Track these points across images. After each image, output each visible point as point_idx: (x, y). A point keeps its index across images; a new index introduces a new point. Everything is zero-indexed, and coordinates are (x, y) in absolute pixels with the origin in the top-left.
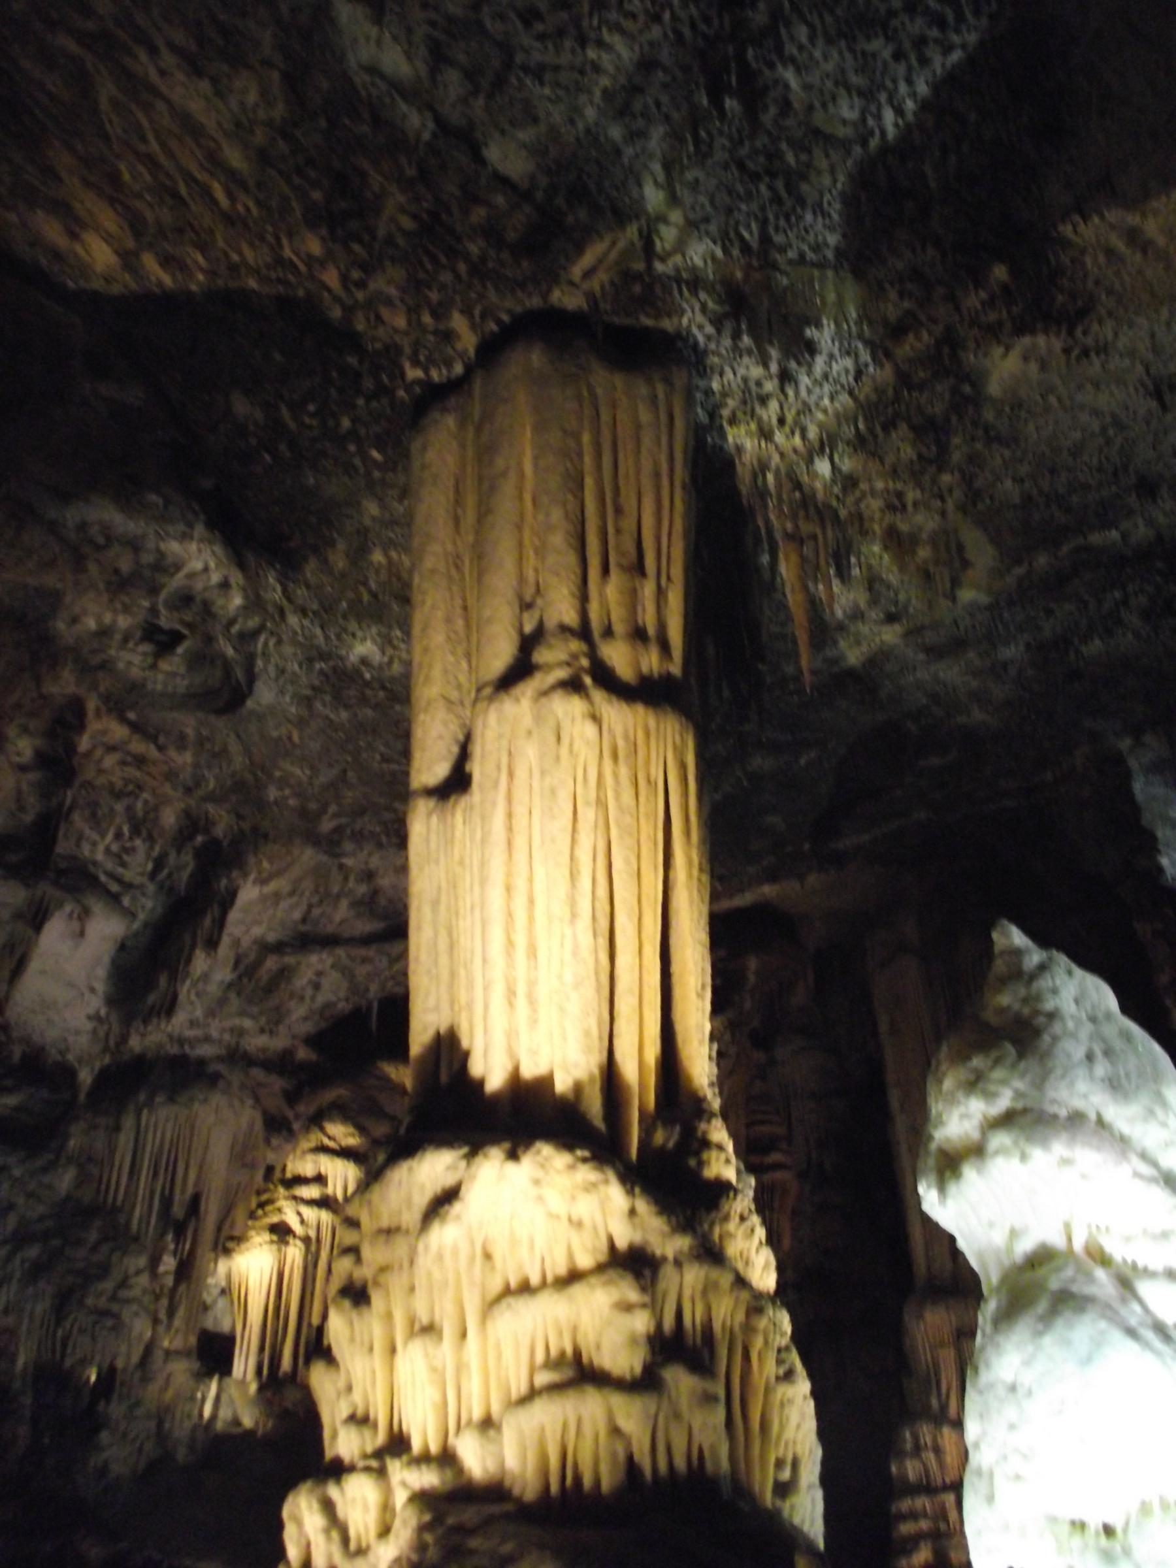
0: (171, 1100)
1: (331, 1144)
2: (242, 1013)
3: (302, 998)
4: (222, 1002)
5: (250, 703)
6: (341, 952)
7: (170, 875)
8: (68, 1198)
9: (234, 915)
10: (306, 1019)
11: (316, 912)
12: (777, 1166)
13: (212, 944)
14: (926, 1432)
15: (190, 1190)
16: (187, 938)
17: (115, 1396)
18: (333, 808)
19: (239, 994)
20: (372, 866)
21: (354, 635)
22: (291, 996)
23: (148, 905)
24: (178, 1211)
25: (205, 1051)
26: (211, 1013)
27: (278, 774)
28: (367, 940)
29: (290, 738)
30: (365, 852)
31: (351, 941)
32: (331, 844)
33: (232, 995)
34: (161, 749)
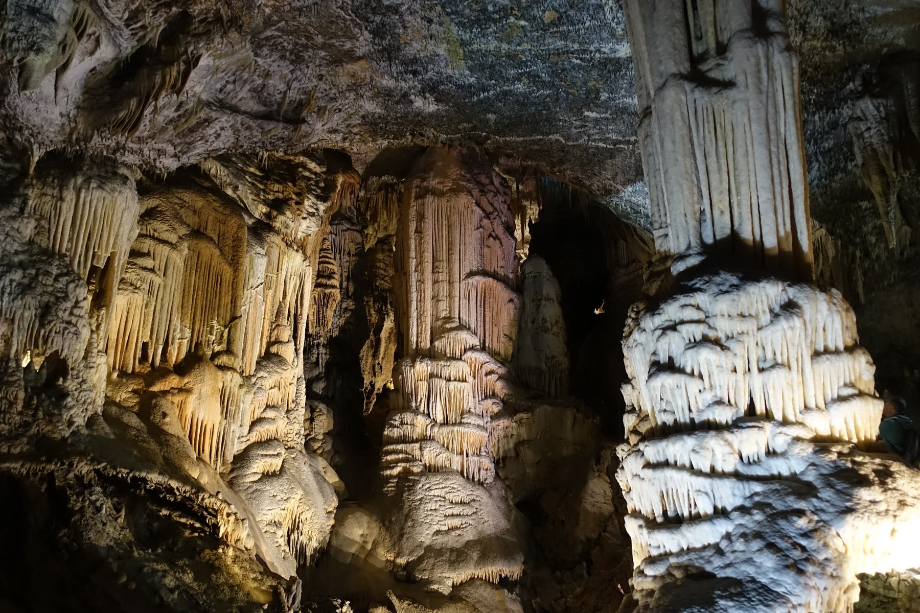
0: (100, 187)
1: (156, 235)
2: (170, 141)
4: (163, 130)
6: (240, 118)
7: (143, 27)
8: (31, 242)
9: (192, 74)
10: (199, 155)
11: (230, 87)
12: (333, 287)
14: (408, 417)
15: (110, 250)
16: (158, 79)
17: (69, 377)
19: (175, 129)
20: (271, 69)
22: (202, 138)
23: (128, 46)
24: (101, 265)
26: (152, 137)
28: (255, 116)
30: (272, 59)
31: (245, 113)
32: (257, 47)
33: (171, 127)
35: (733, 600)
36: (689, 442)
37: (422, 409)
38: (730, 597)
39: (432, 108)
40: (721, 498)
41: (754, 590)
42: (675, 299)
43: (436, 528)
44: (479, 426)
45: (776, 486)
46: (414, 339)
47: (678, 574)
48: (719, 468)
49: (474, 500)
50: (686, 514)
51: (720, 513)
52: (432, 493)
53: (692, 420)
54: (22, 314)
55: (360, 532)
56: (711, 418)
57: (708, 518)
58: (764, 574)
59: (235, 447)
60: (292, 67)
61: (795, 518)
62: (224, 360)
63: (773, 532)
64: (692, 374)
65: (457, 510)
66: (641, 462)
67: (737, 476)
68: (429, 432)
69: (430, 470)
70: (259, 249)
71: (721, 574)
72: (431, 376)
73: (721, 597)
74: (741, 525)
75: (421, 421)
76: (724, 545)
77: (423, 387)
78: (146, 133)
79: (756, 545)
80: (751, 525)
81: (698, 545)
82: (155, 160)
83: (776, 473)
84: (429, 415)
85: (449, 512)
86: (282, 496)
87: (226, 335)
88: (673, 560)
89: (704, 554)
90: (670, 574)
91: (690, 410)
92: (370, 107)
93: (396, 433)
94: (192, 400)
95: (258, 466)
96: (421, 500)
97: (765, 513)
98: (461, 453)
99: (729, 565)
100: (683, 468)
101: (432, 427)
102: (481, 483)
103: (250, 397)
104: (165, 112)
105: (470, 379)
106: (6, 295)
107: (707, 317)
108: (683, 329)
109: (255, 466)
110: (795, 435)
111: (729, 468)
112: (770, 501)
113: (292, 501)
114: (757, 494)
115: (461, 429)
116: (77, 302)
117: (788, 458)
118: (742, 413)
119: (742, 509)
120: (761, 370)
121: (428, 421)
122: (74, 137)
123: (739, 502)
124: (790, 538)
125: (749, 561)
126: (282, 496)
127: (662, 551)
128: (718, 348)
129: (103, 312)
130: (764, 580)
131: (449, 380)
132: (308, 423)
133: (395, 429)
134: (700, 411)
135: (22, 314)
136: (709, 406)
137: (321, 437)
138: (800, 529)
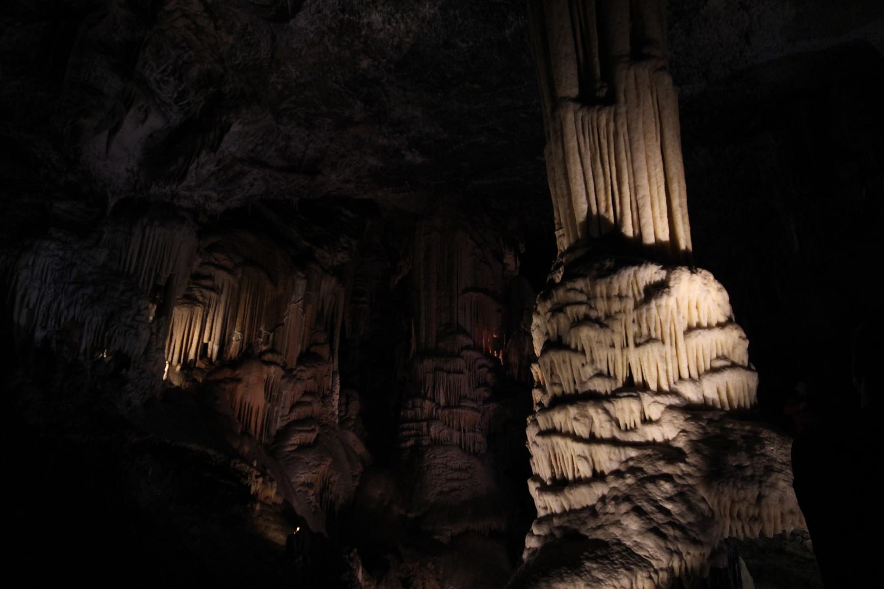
1: (216, 262)
3: (244, 189)
5: (291, 23)
7: (188, 104)
9: (226, 138)
11: (259, 148)
13: (214, 149)
14: (418, 401)
18: (293, 98)
21: (376, 7)
23: (176, 117)
24: (162, 283)
25: (184, 203)
27: (282, 68)
29: (301, 51)
34: (217, 28)
35: (597, 562)
37: (429, 395)
38: (595, 560)
39: (420, 160)
40: (599, 462)
41: (619, 552)
43: (439, 489)
44: (473, 409)
45: (649, 452)
46: (424, 341)
47: (557, 533)
48: (598, 435)
49: (470, 467)
50: (570, 477)
51: (598, 476)
52: (436, 461)
53: (576, 391)
54: (91, 320)
55: (379, 492)
56: (592, 388)
58: (629, 537)
59: (279, 424)
60: (307, 132)
61: (662, 482)
62: (268, 357)
63: (641, 495)
64: (575, 350)
65: (455, 475)
66: (536, 431)
67: (614, 442)
68: (434, 413)
69: (436, 443)
70: (300, 274)
71: (593, 536)
72: (436, 369)
73: (588, 559)
74: (614, 488)
75: (427, 404)
76: (599, 507)
77: (430, 376)
78: (193, 183)
79: (625, 507)
80: (623, 488)
81: (578, 507)
82: (204, 204)
83: (650, 439)
84: (434, 400)
85: (449, 476)
86: (314, 462)
87: (271, 338)
88: (556, 522)
89: (581, 515)
90: (551, 534)
91: (575, 383)
92: (373, 161)
93: (410, 414)
94: (240, 388)
95: (296, 439)
96: (428, 466)
97: (636, 476)
98: (460, 430)
101: (437, 410)
102: (475, 454)
103: (291, 385)
104: (208, 167)
105: (466, 371)
106: (78, 305)
107: (589, 299)
108: (568, 310)
109: (293, 439)
110: (668, 403)
111: (606, 434)
112: (642, 466)
113: (323, 467)
114: (632, 459)
115: (460, 411)
116: (139, 311)
117: (661, 425)
118: (620, 384)
119: (618, 474)
120: (637, 345)
121: (434, 405)
122: (138, 187)
123: (615, 466)
124: (656, 501)
125: (617, 523)
126: (314, 462)
127: (549, 512)
128: (597, 326)
129: (163, 319)
131: (449, 372)
132: (343, 408)
133: (409, 412)
135: (91, 320)
136: (591, 378)
137: (354, 417)
138: (667, 493)
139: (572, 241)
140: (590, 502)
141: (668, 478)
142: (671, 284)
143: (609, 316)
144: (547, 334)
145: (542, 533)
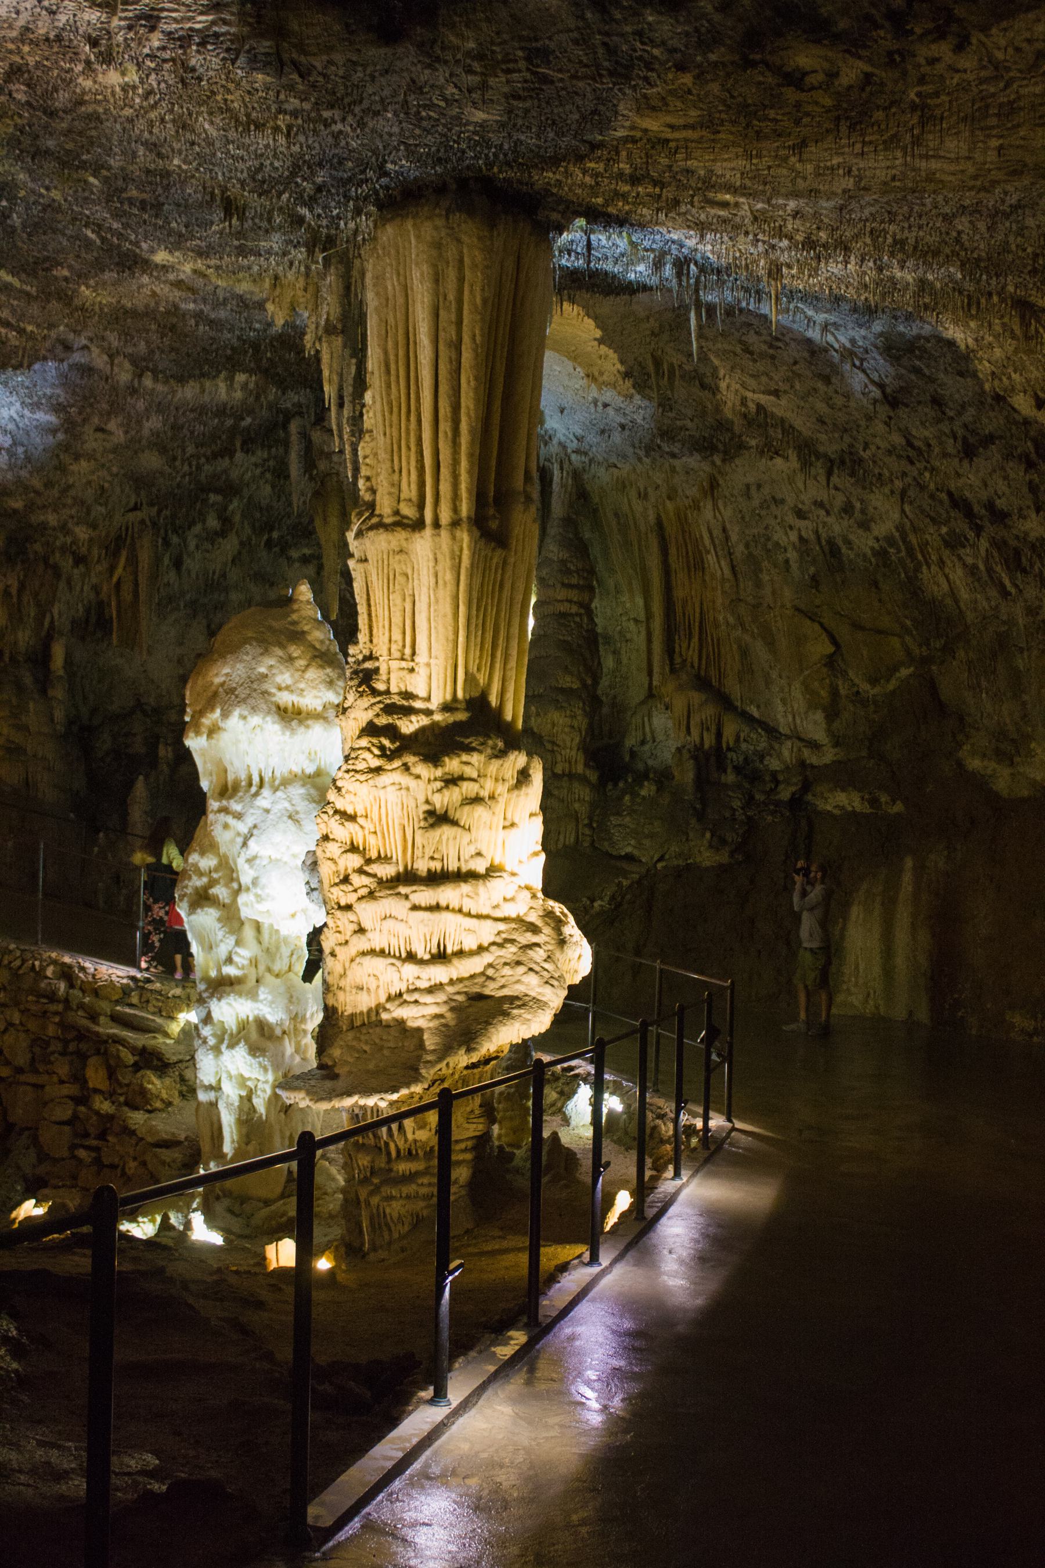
36: (465, 888)
38: (519, 1007)
42: (459, 756)
45: (513, 925)
51: (481, 949)
57: (472, 953)
64: (463, 827)
66: (408, 905)
76: (490, 972)
79: (521, 969)
81: (467, 975)
99: (503, 987)
100: (453, 910)
120: (504, 828)
123: (492, 939)
125: (518, 981)
130: (533, 994)
134: (466, 861)
139: (449, 697)
140: (479, 969)
141: (537, 945)
142: (531, 772)
143: (492, 797)
144: (427, 802)
145: (439, 1000)
